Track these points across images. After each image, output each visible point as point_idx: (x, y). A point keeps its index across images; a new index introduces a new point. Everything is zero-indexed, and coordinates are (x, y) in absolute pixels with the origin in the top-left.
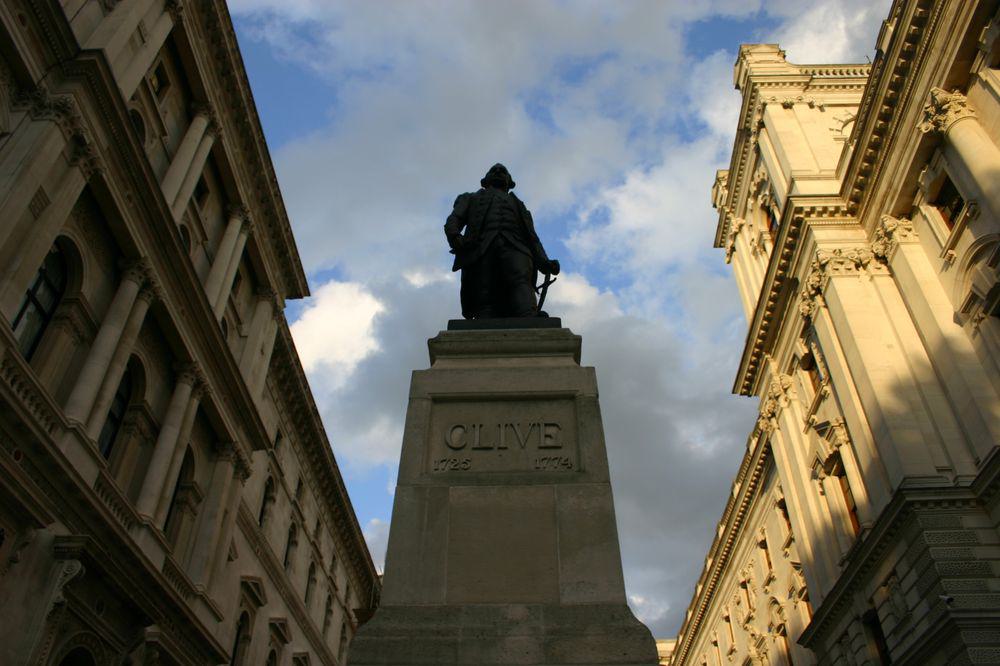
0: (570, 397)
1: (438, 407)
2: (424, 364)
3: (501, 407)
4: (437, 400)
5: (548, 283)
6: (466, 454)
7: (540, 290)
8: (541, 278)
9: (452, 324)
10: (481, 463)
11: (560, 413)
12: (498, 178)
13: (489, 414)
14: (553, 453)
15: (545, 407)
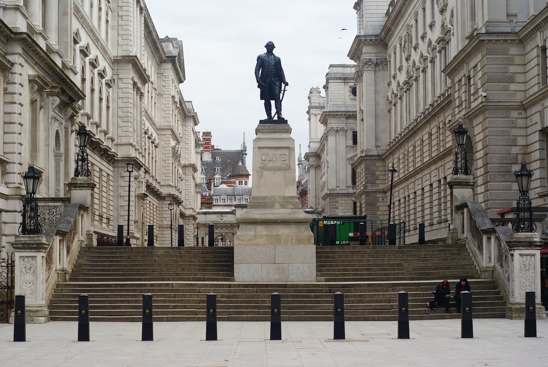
0: (289, 148)
1: (260, 149)
2: (255, 136)
3: (273, 150)
4: (259, 148)
5: (284, 91)
6: (266, 162)
7: (282, 92)
8: (283, 85)
9: (261, 122)
10: (270, 165)
11: (286, 152)
12: (270, 47)
13: (271, 152)
14: (284, 162)
15: (283, 150)
